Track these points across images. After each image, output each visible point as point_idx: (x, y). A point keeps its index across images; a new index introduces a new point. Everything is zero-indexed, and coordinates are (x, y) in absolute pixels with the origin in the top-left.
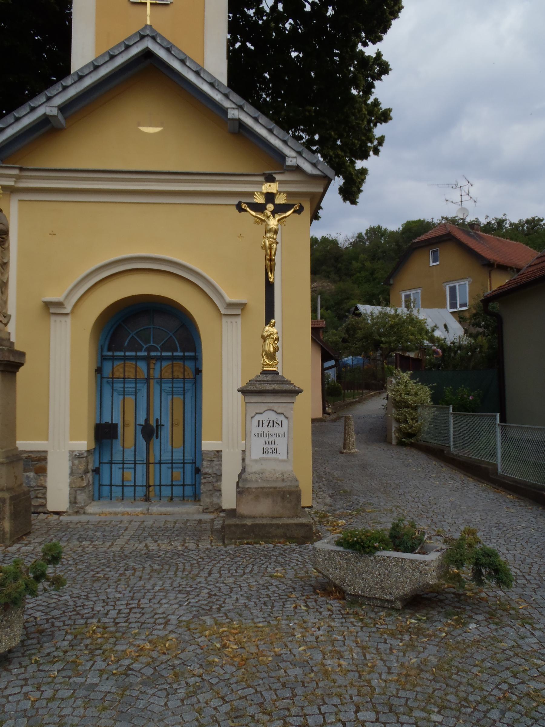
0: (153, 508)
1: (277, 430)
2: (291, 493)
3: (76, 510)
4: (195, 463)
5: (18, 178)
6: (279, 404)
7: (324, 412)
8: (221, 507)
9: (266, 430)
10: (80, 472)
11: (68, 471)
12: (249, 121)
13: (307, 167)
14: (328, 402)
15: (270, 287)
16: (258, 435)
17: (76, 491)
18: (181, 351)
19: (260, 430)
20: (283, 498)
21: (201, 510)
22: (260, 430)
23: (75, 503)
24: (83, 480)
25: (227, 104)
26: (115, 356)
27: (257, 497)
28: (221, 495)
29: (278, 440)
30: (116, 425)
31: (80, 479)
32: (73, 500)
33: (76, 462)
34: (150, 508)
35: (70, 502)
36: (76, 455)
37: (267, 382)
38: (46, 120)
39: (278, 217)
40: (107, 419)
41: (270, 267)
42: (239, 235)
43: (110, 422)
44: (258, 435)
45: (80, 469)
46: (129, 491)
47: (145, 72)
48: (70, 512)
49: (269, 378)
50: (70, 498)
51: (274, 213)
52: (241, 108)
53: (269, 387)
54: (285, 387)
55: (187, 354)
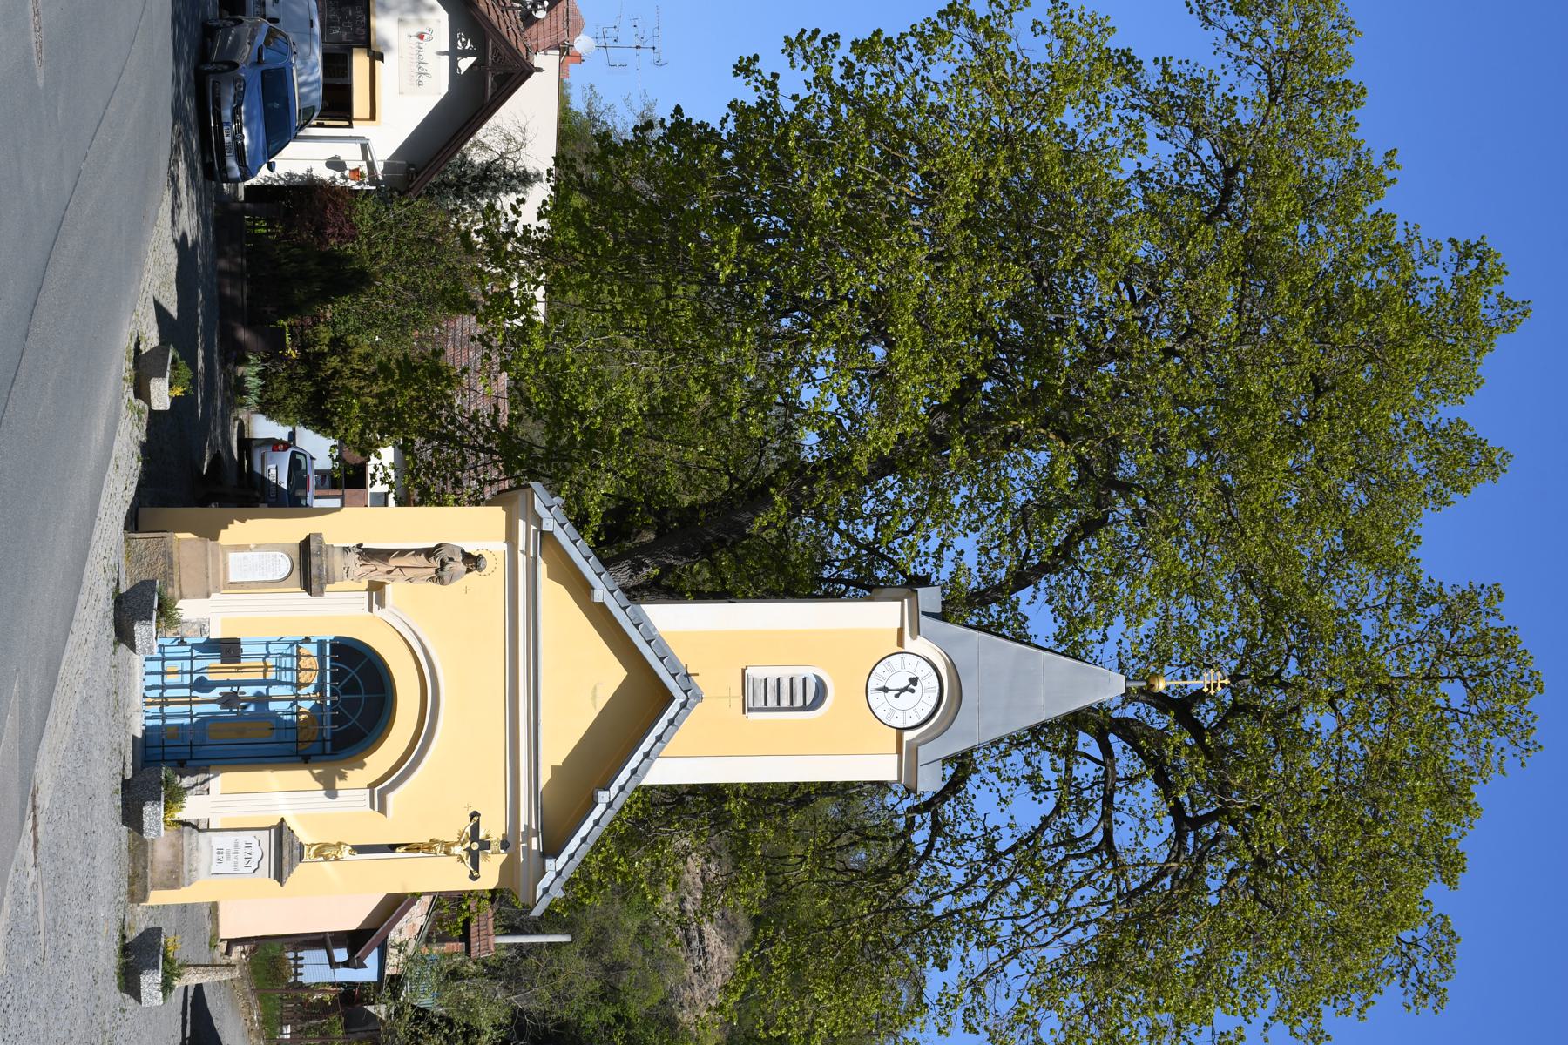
1: (242, 862)
2: (177, 879)
5: (526, 553)
6: (267, 865)
7: (232, 943)
9: (242, 850)
12: (596, 814)
13: (545, 882)
14: (252, 951)
15: (392, 848)
16: (236, 843)
18: (333, 734)
19: (242, 845)
20: (172, 872)
22: (242, 845)
25: (614, 789)
27: (174, 846)
29: (231, 863)
37: (291, 851)
38: (589, 588)
39: (464, 855)
40: (246, 649)
41: (411, 848)
44: (236, 843)
46: (156, 680)
47: (647, 699)
49: (296, 852)
51: (469, 850)
52: (610, 805)
53: (286, 852)
54: (286, 869)
55: (328, 744)
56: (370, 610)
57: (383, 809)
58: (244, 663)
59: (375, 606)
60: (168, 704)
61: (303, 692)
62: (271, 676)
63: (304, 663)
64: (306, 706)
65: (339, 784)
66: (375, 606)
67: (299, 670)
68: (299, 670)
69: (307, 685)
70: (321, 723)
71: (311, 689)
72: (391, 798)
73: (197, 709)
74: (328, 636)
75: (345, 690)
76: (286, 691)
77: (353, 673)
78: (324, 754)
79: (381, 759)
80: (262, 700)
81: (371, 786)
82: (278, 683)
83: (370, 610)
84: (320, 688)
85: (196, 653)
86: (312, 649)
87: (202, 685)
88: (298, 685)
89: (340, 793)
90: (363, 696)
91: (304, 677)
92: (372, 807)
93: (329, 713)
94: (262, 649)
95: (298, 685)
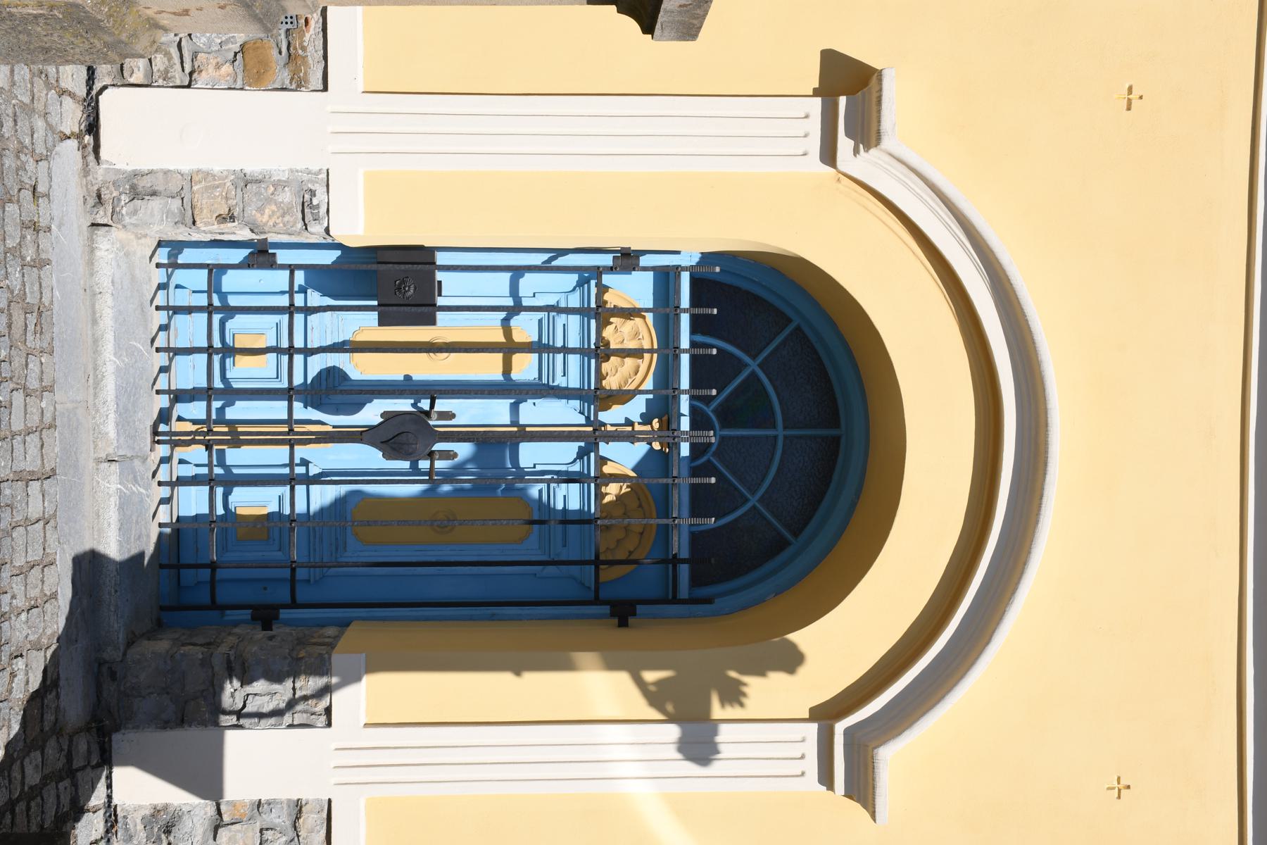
0: (114, 478)
3: (106, 196)
4: (294, 604)
8: (117, 730)
10: (251, 211)
11: (252, 167)
17: (179, 195)
18: (696, 538)
21: (106, 656)
23: (135, 194)
24: (222, 219)
26: (677, 317)
28: (166, 725)
30: (431, 321)
31: (224, 211)
32: (144, 183)
33: (287, 197)
34: (114, 466)
35: (136, 174)
36: (313, 193)
40: (452, 287)
42: (1124, 782)
43: (440, 301)
45: (261, 210)
46: (190, 373)
48: (99, 173)
50: (151, 172)
55: (684, 570)
56: (829, 155)
57: (862, 788)
58: (447, 327)
59: (845, 144)
60: (236, 442)
61: (613, 416)
62: (525, 368)
63: (620, 333)
64: (623, 457)
65: (718, 711)
66: (845, 144)
67: (602, 352)
68: (602, 352)
69: (622, 396)
70: (666, 513)
71: (635, 408)
72: (892, 759)
73: (322, 457)
74: (692, 236)
75: (728, 415)
76: (566, 413)
77: (753, 365)
78: (675, 600)
79: (845, 638)
80: (495, 445)
81: (825, 714)
82: (542, 390)
83: (829, 155)
84: (662, 408)
85: (315, 299)
86: (634, 289)
87: (332, 390)
88: (599, 397)
89: (726, 734)
90: (780, 432)
91: (617, 374)
92: (826, 778)
93: (685, 482)
94: (496, 288)
95: (599, 397)
